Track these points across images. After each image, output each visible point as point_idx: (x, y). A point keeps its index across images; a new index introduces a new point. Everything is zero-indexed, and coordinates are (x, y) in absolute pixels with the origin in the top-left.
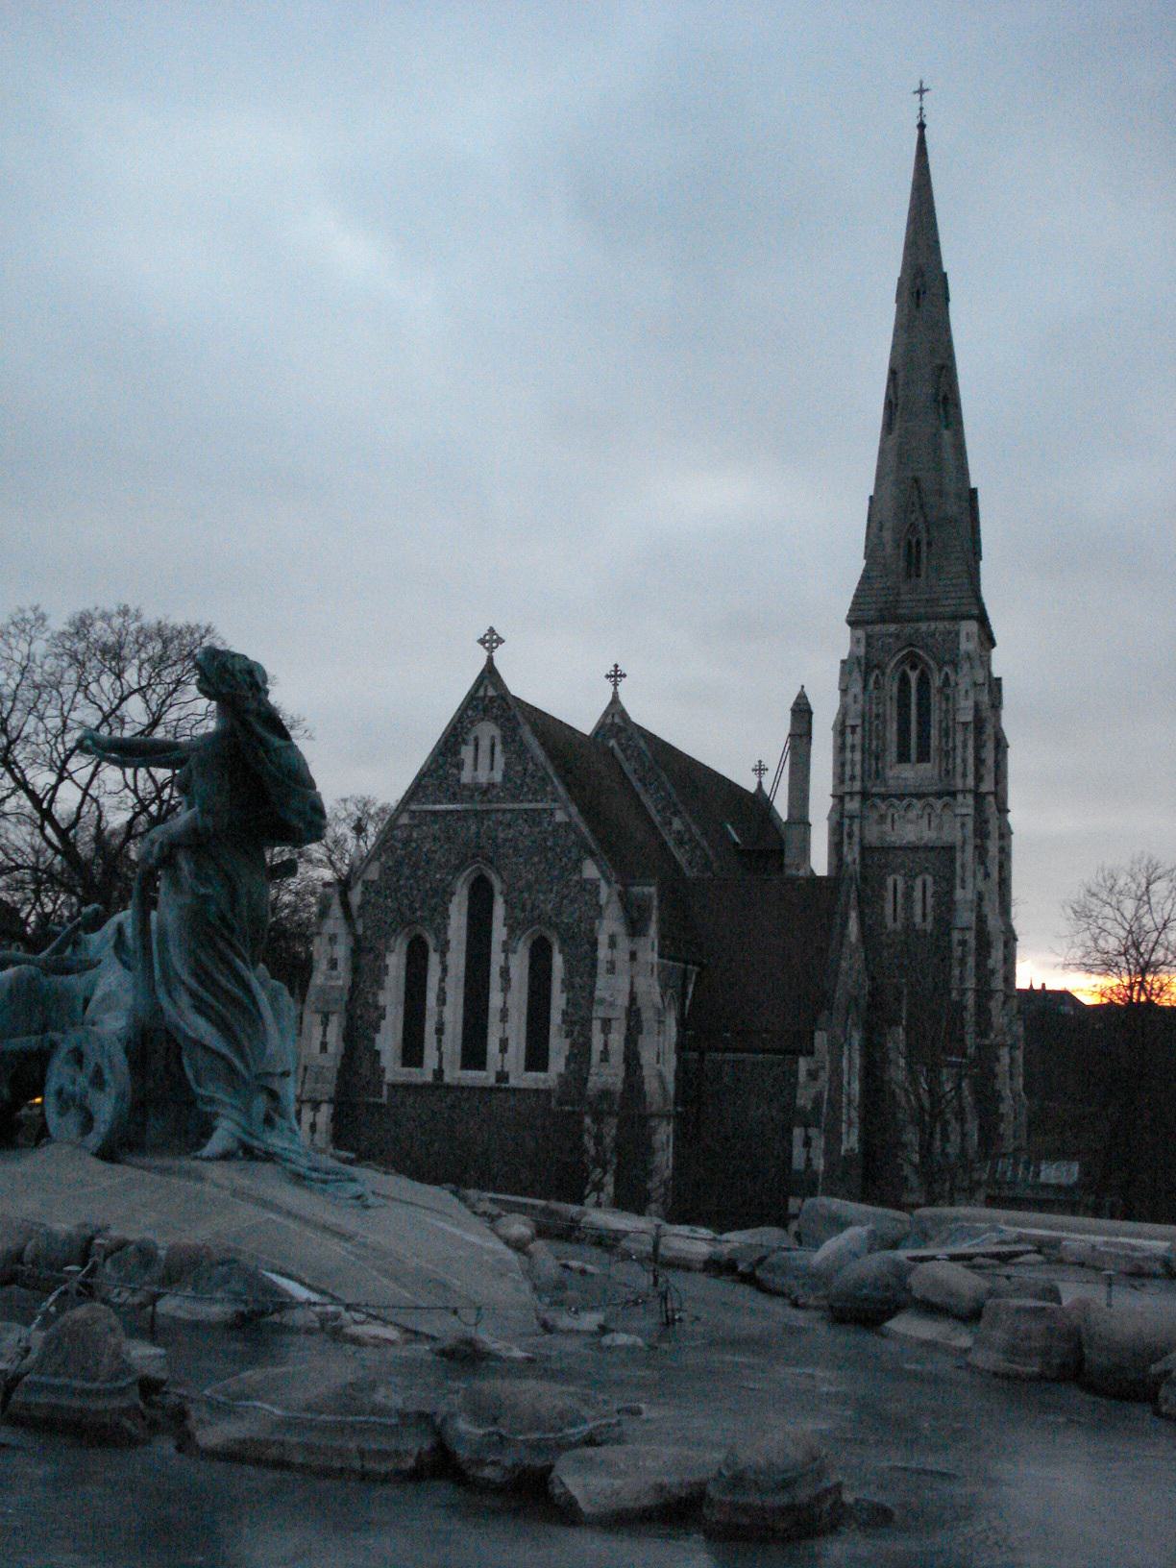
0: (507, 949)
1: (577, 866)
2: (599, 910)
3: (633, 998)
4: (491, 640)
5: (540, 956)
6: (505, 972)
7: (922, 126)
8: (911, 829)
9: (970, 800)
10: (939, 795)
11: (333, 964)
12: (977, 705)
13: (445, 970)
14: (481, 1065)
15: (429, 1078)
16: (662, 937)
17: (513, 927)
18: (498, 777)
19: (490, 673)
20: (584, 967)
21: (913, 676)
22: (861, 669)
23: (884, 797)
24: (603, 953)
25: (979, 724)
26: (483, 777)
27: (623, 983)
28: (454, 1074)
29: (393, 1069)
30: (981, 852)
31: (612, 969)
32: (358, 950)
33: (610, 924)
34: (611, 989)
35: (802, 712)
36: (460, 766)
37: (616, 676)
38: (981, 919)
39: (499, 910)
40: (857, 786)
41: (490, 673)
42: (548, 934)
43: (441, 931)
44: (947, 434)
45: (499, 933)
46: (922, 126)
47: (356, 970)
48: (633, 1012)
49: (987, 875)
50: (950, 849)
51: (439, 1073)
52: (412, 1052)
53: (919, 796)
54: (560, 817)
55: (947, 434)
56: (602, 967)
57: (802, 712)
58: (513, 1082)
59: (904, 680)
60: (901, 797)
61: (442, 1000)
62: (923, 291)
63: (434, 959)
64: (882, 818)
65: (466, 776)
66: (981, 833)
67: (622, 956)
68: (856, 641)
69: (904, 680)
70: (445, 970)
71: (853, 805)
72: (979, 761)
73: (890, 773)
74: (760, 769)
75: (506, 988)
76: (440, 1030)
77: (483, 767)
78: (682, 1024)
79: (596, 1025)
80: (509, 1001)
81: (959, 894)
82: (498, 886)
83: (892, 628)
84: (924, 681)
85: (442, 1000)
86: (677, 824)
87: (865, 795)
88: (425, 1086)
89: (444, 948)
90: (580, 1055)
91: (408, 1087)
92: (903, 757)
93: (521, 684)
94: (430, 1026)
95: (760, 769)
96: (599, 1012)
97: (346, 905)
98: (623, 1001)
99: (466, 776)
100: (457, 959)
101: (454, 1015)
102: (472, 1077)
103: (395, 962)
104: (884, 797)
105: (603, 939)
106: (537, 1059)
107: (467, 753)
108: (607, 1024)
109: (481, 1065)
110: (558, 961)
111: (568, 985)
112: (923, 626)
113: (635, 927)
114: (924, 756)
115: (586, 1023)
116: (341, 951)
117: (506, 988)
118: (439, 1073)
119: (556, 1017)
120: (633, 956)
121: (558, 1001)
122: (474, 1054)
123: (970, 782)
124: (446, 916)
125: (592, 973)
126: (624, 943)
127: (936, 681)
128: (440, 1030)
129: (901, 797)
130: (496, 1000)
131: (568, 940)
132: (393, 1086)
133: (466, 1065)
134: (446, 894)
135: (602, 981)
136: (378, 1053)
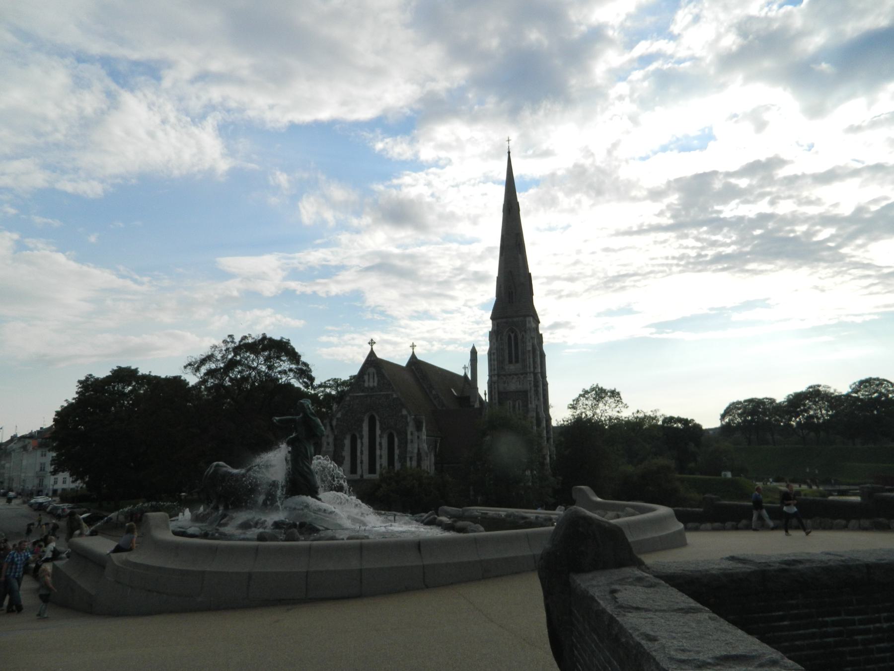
0: (381, 437)
2: (407, 424)
3: (419, 449)
4: (372, 343)
6: (380, 444)
7: (509, 153)
8: (513, 386)
9: (532, 375)
10: (522, 374)
11: (328, 444)
12: (533, 346)
13: (362, 443)
14: (375, 473)
16: (427, 430)
17: (382, 429)
18: (376, 384)
19: (372, 353)
20: (404, 443)
21: (512, 336)
22: (495, 335)
23: (504, 375)
24: (409, 437)
25: (534, 350)
26: (371, 385)
27: (416, 446)
28: (367, 476)
30: (537, 392)
31: (412, 442)
32: (335, 439)
33: (411, 428)
34: (413, 448)
35: (474, 353)
36: (364, 381)
37: (413, 346)
38: (537, 413)
39: (378, 423)
40: (496, 372)
41: (372, 353)
43: (361, 431)
44: (520, 256)
45: (378, 432)
46: (509, 153)
47: (335, 445)
48: (419, 454)
49: (539, 399)
50: (525, 393)
51: (362, 476)
53: (516, 375)
54: (395, 396)
55: (520, 256)
56: (409, 441)
57: (474, 353)
59: (510, 337)
60: (510, 375)
61: (362, 453)
62: (511, 210)
63: (359, 441)
64: (504, 383)
65: (366, 385)
66: (536, 386)
68: (493, 324)
69: (510, 337)
70: (362, 443)
71: (495, 379)
72: (534, 362)
73: (506, 367)
74: (465, 368)
75: (381, 449)
76: (362, 462)
77: (371, 382)
78: (435, 456)
79: (408, 459)
80: (382, 453)
81: (530, 406)
82: (377, 418)
83: (504, 320)
84: (516, 337)
85: (362, 453)
86: (434, 392)
87: (499, 375)
89: (362, 438)
92: (510, 362)
93: (380, 355)
94: (359, 461)
95: (465, 368)
96: (408, 455)
97: (331, 426)
98: (416, 451)
99: (366, 385)
100: (366, 440)
101: (366, 458)
102: (372, 476)
103: (347, 442)
104: (504, 375)
105: (409, 433)
107: (366, 377)
108: (411, 459)
109: (375, 473)
110: (396, 440)
111: (399, 447)
112: (515, 320)
113: (419, 428)
114: (517, 362)
115: (405, 458)
116: (331, 440)
117: (381, 449)
118: (362, 476)
119: (396, 457)
120: (418, 437)
121: (397, 452)
123: (532, 369)
124: (362, 428)
125: (406, 443)
126: (416, 434)
127: (520, 337)
128: (362, 462)
129: (510, 375)
130: (378, 452)
133: (370, 473)
134: (362, 421)
135: (409, 446)
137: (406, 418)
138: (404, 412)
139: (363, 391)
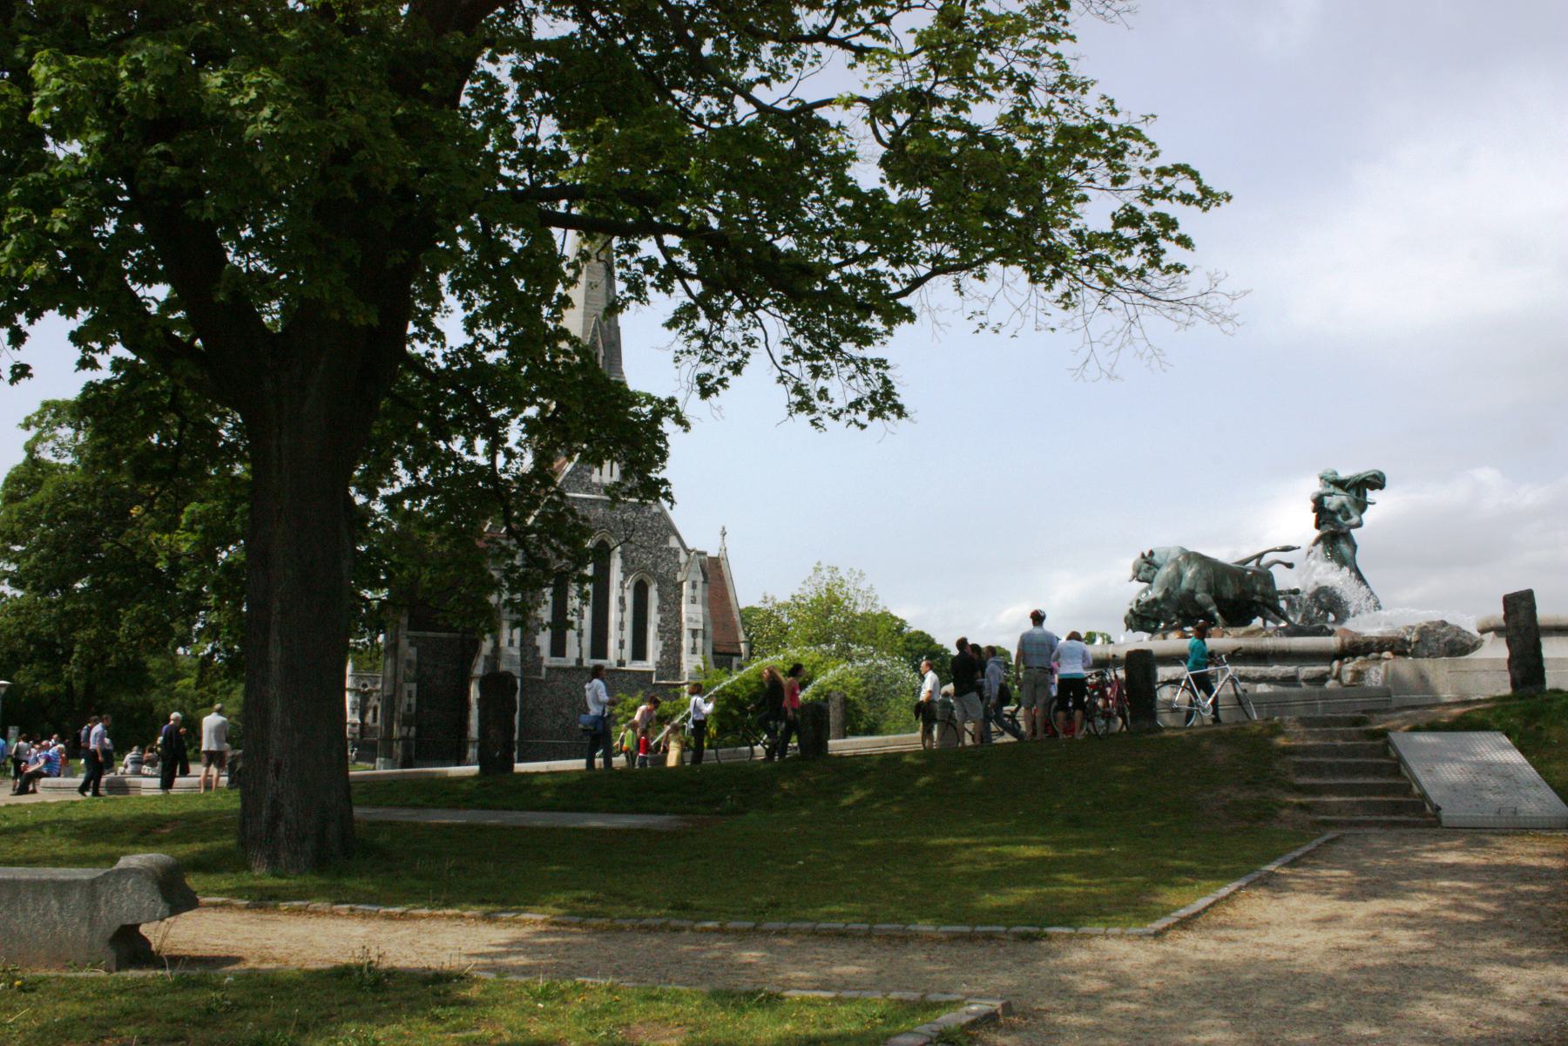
1: (666, 541)
5: (641, 592)
15: (573, 663)
29: (548, 661)
42: (647, 578)
51: (580, 661)
52: (558, 648)
58: (628, 667)
67: (699, 592)
75: (622, 611)
80: (618, 617)
88: (572, 668)
90: (672, 651)
91: (559, 669)
106: (639, 652)
111: (661, 610)
117: (622, 611)
118: (580, 661)
121: (654, 618)
122: (599, 648)
130: (614, 616)
131: (663, 582)
132: (549, 669)
136: (538, 648)
137: (676, 554)
138: (673, 542)
139: (588, 490)
